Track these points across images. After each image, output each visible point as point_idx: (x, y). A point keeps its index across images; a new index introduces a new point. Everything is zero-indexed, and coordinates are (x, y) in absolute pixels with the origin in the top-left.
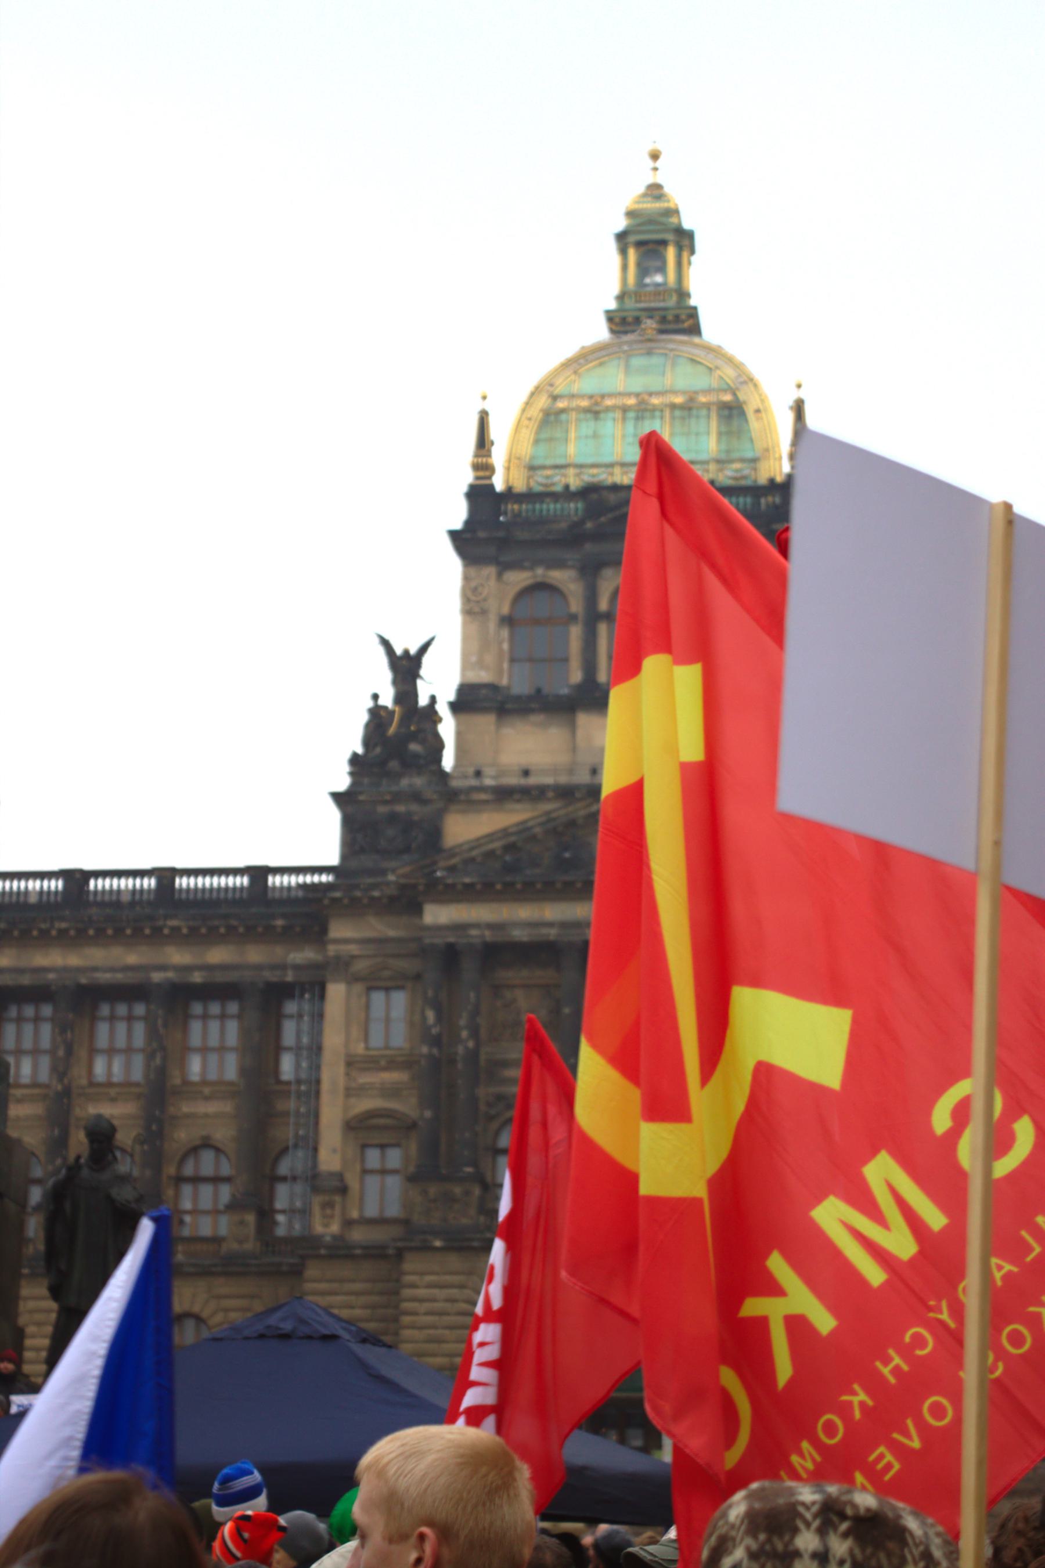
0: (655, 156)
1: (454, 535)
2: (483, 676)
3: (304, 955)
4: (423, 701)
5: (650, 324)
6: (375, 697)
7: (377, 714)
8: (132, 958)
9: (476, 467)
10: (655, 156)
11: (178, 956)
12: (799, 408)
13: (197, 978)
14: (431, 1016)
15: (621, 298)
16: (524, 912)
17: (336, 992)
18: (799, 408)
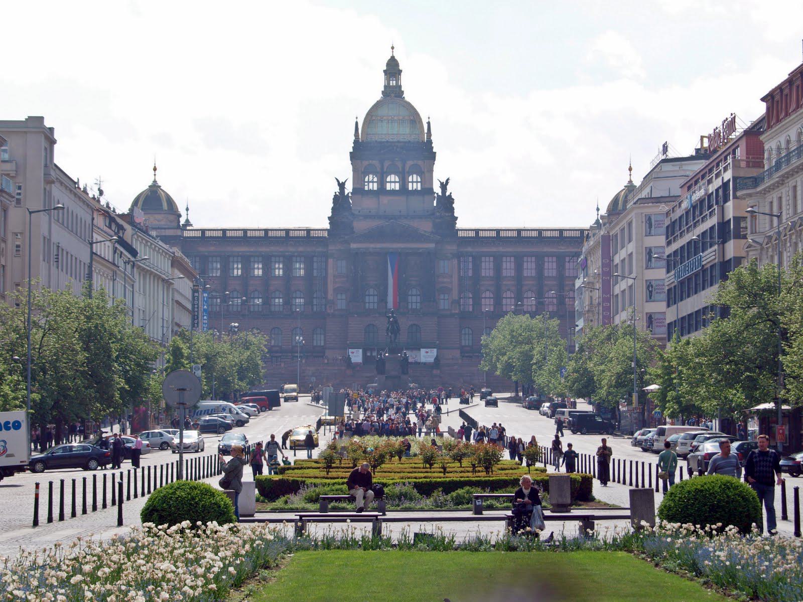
0: (393, 48)
1: (351, 153)
2: (358, 186)
3: (320, 249)
4: (346, 194)
5: (393, 95)
6: (336, 193)
7: (336, 196)
8: (281, 250)
9: (355, 136)
10: (393, 48)
11: (291, 249)
12: (429, 123)
13: (296, 254)
14: (352, 268)
15: (385, 87)
16: (372, 246)
17: (331, 261)
18: (429, 123)
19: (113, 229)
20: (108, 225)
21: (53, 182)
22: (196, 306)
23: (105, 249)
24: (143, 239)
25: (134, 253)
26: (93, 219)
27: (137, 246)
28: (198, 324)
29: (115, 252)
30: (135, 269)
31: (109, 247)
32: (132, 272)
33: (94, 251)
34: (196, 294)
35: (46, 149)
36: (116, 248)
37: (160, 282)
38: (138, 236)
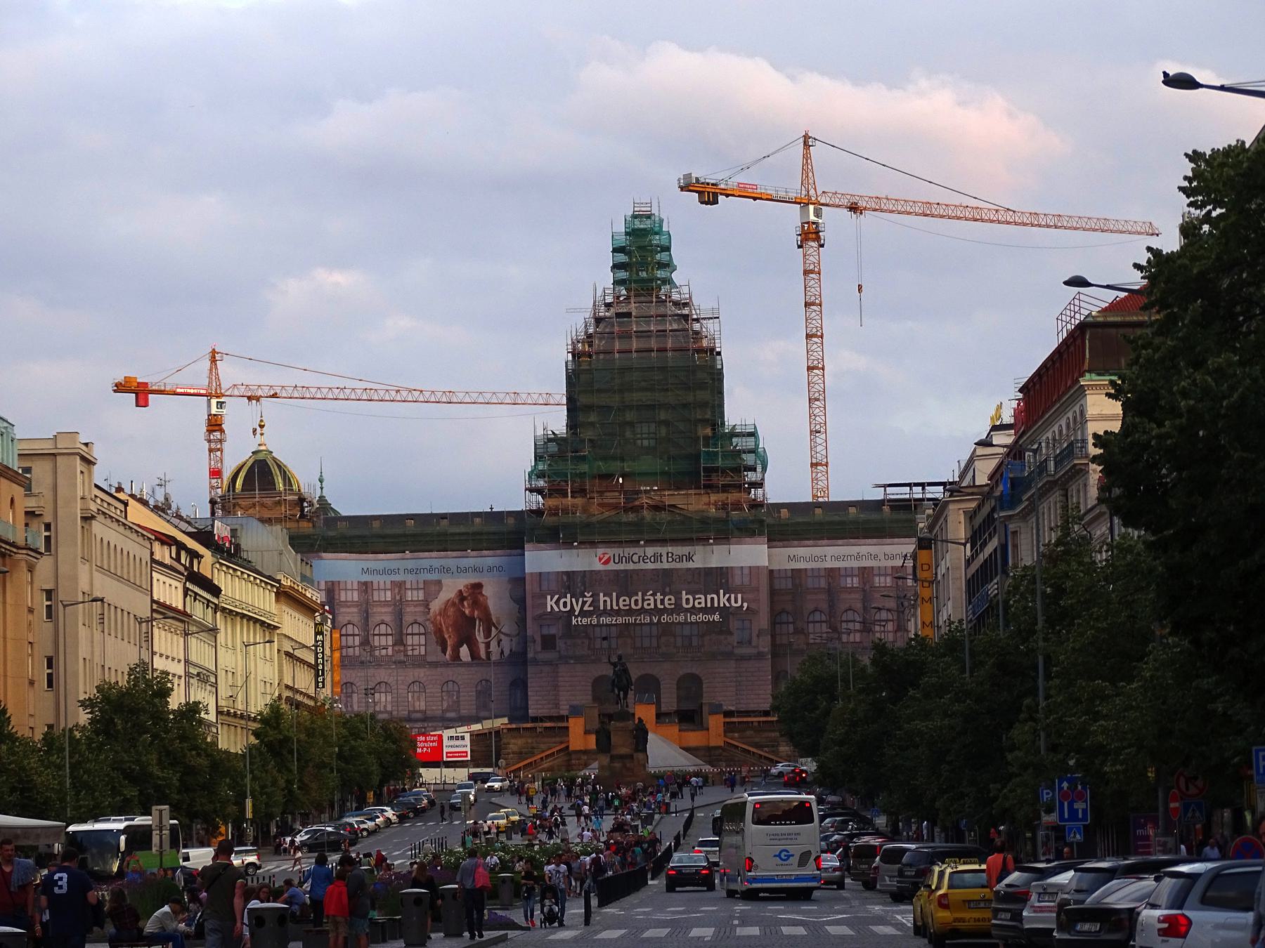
19: (183, 561)
20: (174, 555)
21: (93, 517)
22: (320, 656)
23: (169, 591)
24: (228, 567)
25: (216, 591)
26: (152, 554)
27: (221, 580)
28: (323, 682)
29: (185, 595)
30: (218, 614)
31: (176, 588)
32: (215, 618)
33: (155, 598)
34: (319, 638)
35: (82, 472)
36: (188, 589)
37: (258, 625)
38: (221, 564)
